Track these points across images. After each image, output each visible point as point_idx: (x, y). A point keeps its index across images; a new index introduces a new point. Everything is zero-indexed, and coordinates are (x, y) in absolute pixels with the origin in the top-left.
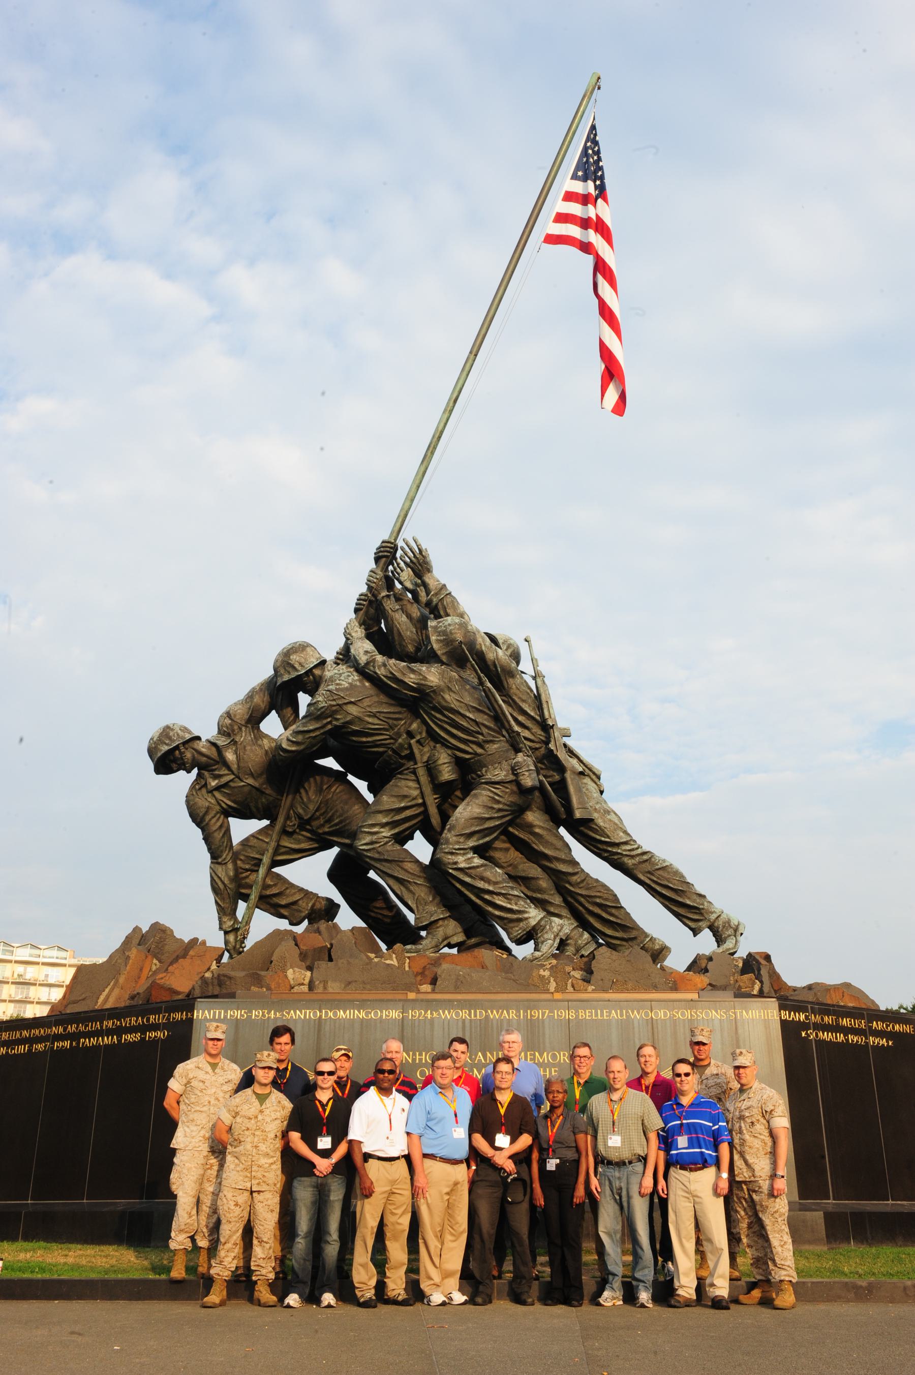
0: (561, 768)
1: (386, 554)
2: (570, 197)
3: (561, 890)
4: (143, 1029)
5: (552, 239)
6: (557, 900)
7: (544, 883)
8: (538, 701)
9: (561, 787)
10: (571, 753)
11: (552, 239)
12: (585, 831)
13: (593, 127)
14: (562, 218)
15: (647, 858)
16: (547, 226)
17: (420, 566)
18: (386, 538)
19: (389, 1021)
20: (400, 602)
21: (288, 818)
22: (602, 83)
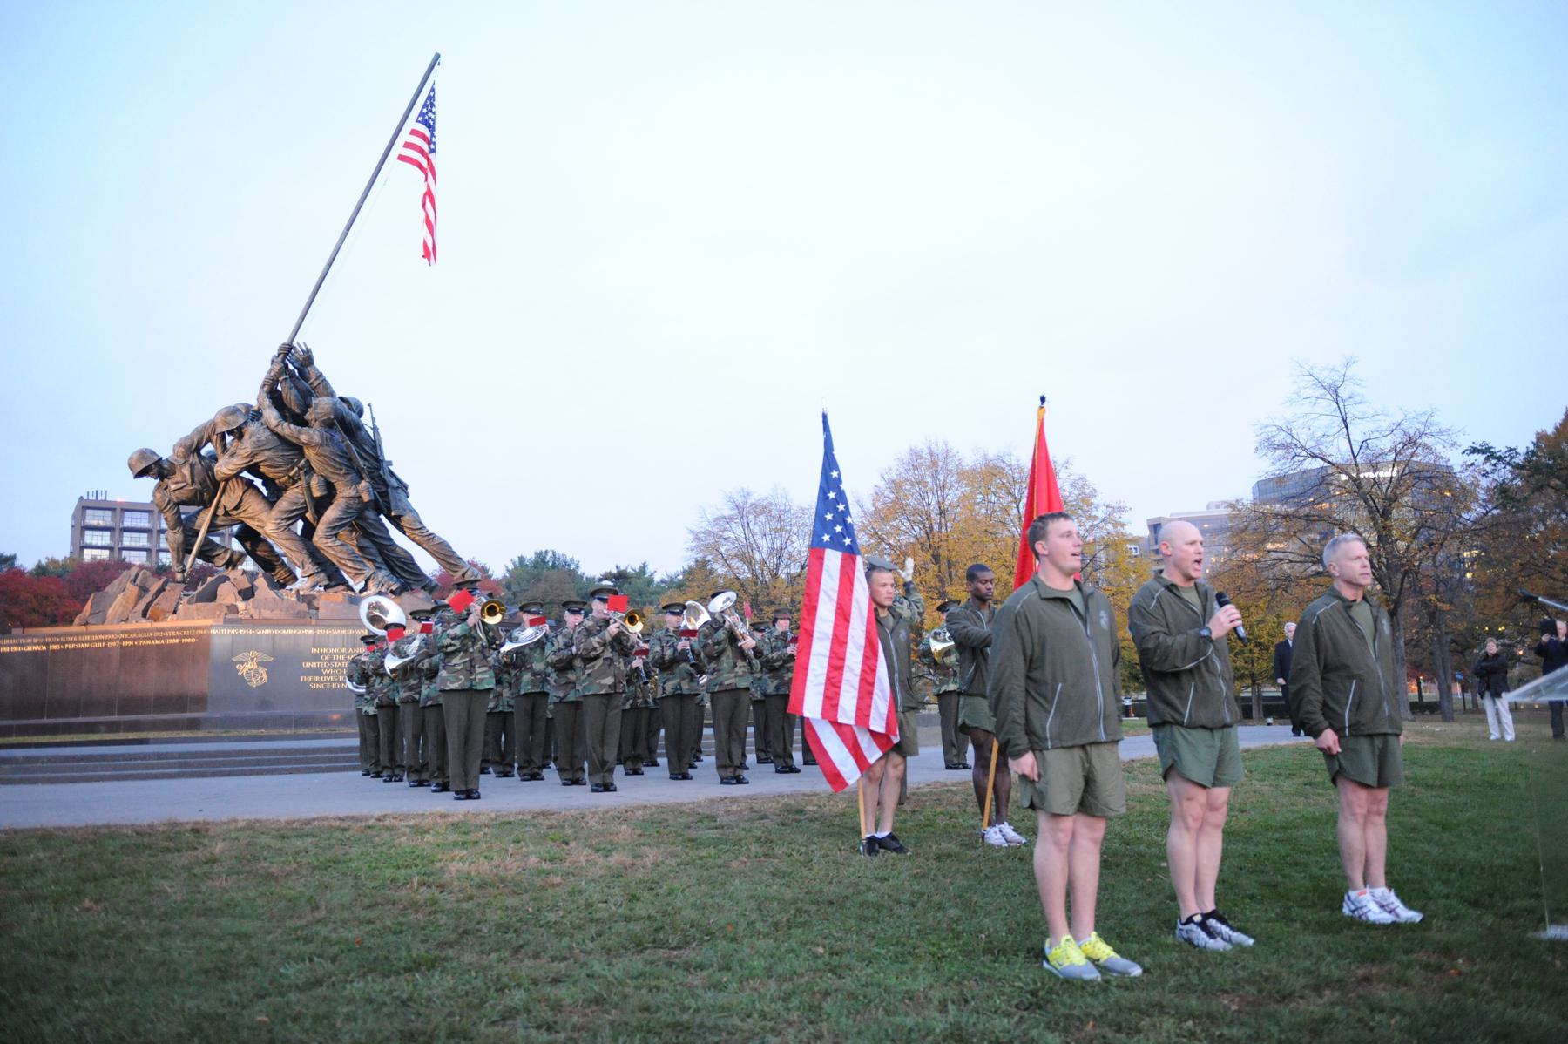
0: (386, 485)
1: (287, 350)
2: (414, 132)
3: (381, 554)
4: (180, 637)
5: (401, 158)
6: (380, 559)
7: (374, 550)
8: (375, 445)
9: (385, 495)
10: (392, 474)
11: (401, 158)
12: (396, 521)
13: (433, 90)
14: (408, 145)
15: (431, 537)
16: (398, 149)
17: (308, 360)
18: (286, 340)
19: (306, 636)
20: (294, 381)
21: (217, 507)
22: (441, 60)
